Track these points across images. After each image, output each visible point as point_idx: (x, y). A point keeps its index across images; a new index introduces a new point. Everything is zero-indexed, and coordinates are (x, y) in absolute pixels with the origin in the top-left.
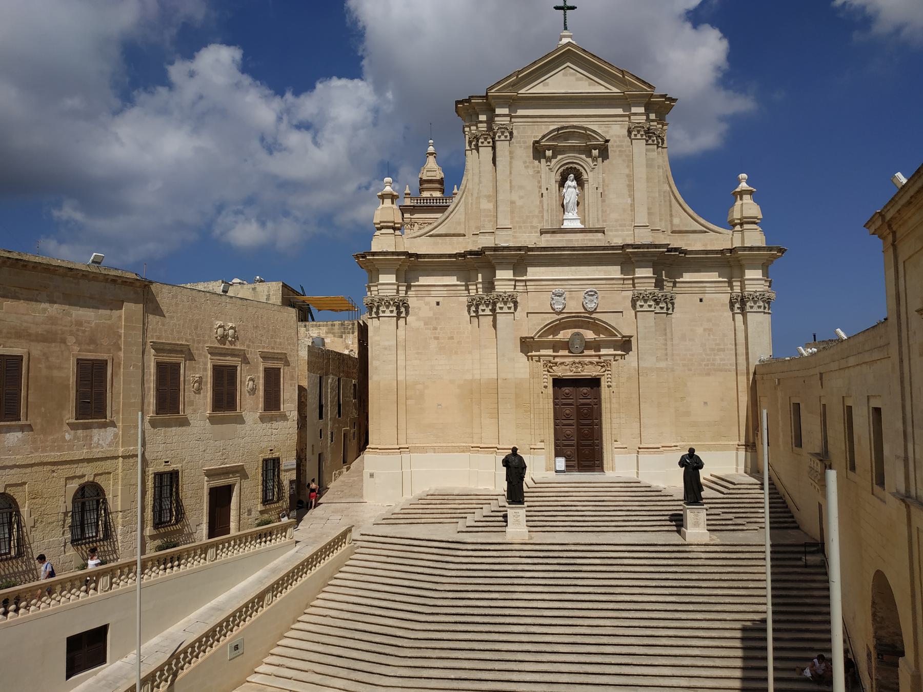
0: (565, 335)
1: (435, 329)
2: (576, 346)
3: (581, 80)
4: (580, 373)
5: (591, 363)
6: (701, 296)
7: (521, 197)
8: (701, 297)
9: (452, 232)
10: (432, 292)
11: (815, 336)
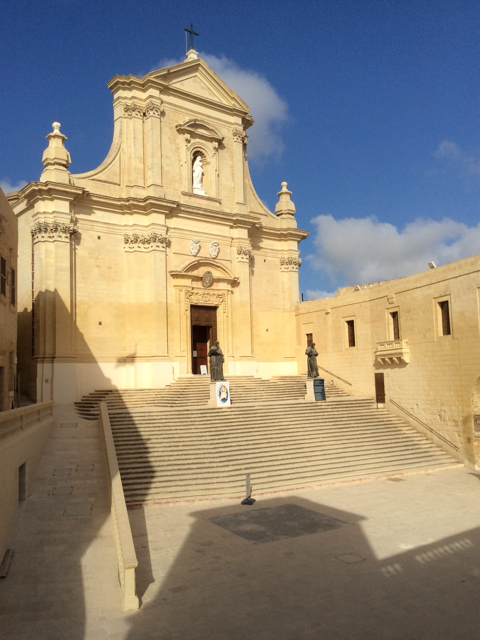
0: (201, 272)
1: (97, 258)
2: (206, 282)
3: (204, 89)
4: (207, 301)
5: (214, 294)
6: (265, 258)
7: (168, 165)
8: (265, 259)
9: (110, 181)
10: (95, 227)
11: (302, 295)
